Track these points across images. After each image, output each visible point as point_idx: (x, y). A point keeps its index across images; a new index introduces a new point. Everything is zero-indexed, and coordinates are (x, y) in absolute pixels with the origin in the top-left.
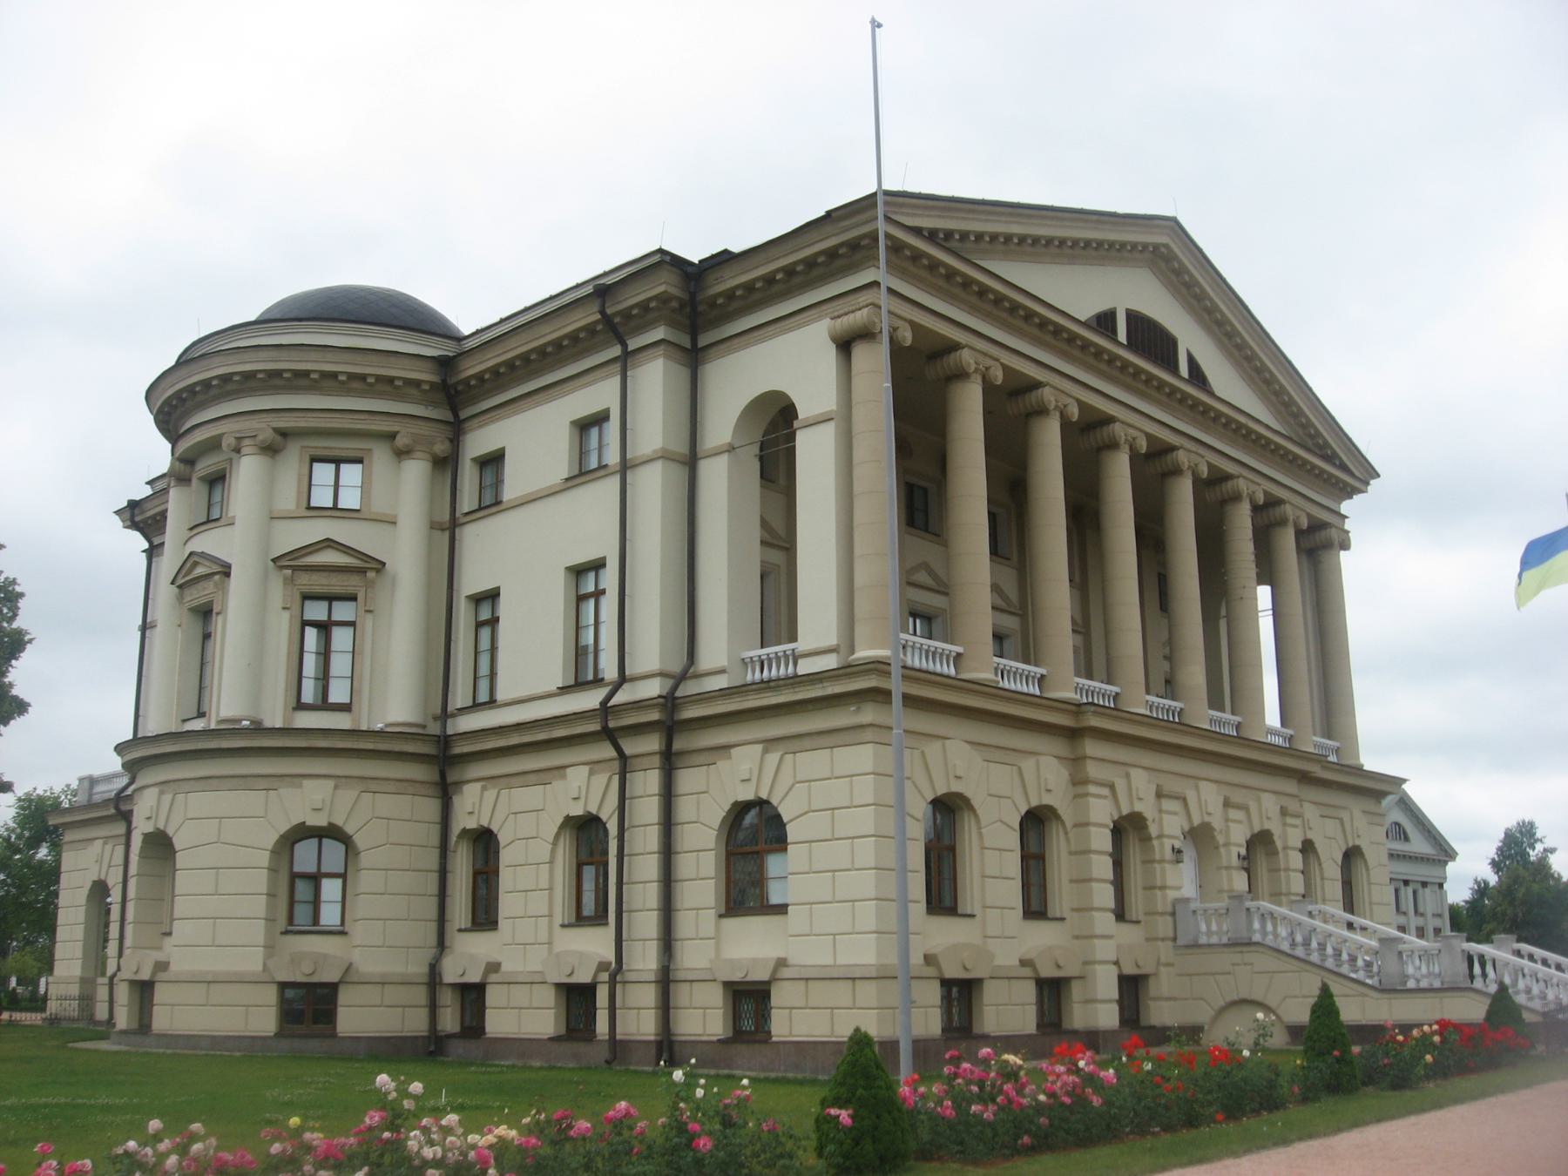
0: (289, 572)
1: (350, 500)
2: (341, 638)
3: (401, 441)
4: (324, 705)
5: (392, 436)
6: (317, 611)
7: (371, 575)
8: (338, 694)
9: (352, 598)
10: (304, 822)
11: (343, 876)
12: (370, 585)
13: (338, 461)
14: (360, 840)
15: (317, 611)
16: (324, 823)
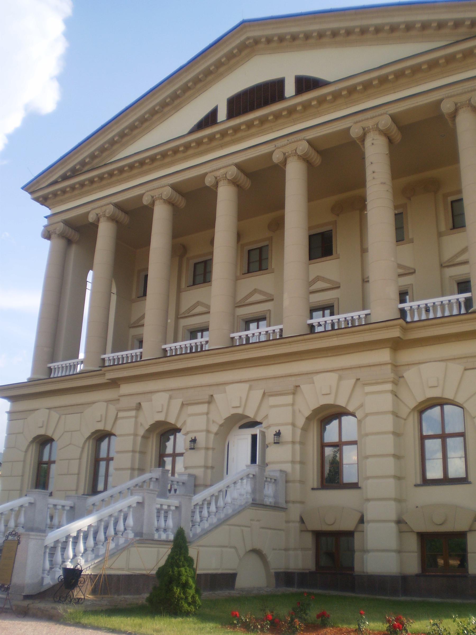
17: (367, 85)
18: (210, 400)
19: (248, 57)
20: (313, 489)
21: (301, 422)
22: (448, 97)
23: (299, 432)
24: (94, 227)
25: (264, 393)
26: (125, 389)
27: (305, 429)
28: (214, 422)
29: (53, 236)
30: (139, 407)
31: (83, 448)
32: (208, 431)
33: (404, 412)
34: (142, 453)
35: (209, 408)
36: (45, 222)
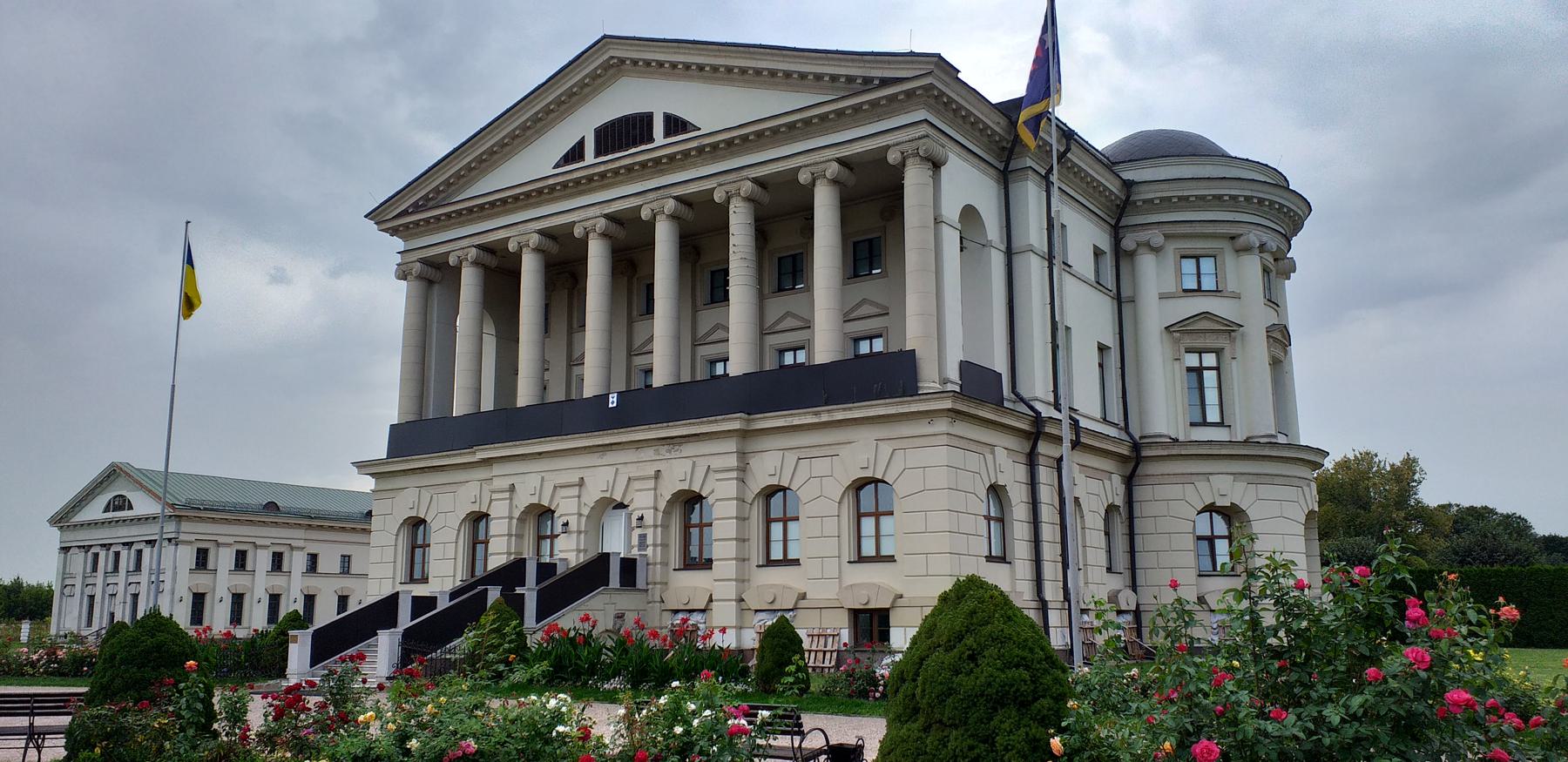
0: (1178, 334)
1: (1208, 283)
2: (1210, 378)
3: (1241, 241)
4: (1205, 423)
5: (1233, 238)
6: (1192, 360)
7: (1233, 334)
8: (1213, 415)
9: (1218, 352)
10: (1214, 503)
11: (1230, 538)
12: (1232, 340)
13: (1197, 258)
14: (1252, 514)
15: (1192, 360)
16: (1229, 505)
17: (730, 143)
18: (581, 483)
19: (615, 77)
20: (674, 570)
21: (662, 505)
22: (805, 166)
23: (660, 515)
24: (457, 271)
25: (629, 478)
26: (497, 470)
27: (667, 512)
28: (585, 504)
29: (409, 277)
30: (512, 488)
31: (459, 531)
32: (580, 515)
33: (750, 497)
34: (519, 536)
35: (580, 491)
36: (398, 259)
